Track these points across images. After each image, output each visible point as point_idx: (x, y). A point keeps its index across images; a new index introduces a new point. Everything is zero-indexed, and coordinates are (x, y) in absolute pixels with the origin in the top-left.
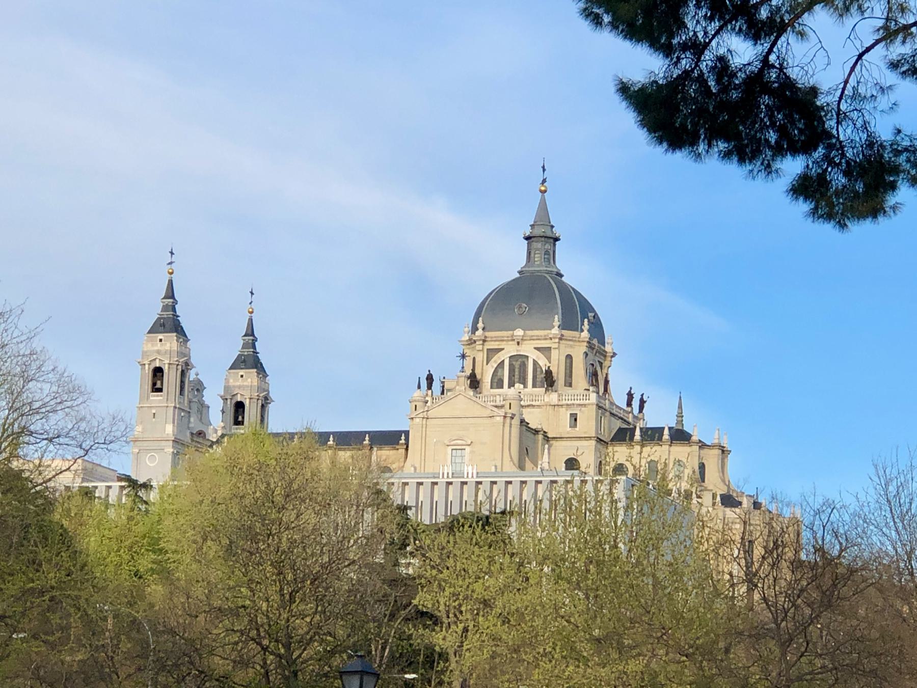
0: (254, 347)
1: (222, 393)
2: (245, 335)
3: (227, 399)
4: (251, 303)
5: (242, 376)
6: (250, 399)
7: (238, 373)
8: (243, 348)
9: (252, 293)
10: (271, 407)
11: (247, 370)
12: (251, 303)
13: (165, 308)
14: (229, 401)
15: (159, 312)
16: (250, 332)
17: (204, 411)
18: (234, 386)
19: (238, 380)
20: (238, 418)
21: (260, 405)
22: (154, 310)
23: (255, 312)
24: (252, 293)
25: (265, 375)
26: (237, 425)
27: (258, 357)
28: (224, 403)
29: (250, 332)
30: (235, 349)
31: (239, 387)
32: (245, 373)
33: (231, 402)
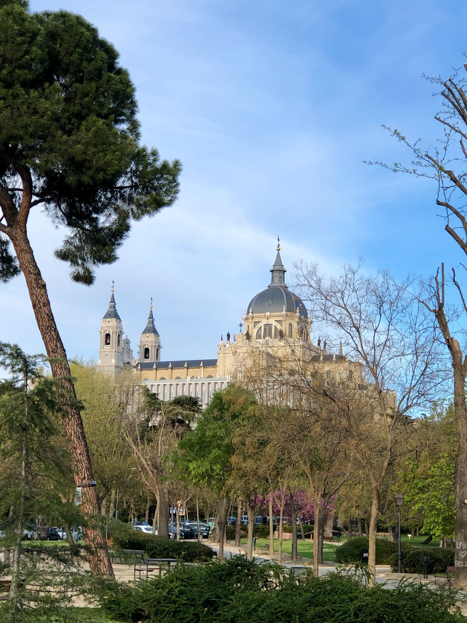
0: (153, 323)
2: (149, 318)
9: (152, 299)
10: (161, 350)
13: (111, 307)
14: (142, 348)
15: (108, 309)
16: (151, 317)
18: (144, 341)
24: (152, 299)
25: (158, 336)
29: (151, 317)
30: (145, 324)
31: (147, 341)
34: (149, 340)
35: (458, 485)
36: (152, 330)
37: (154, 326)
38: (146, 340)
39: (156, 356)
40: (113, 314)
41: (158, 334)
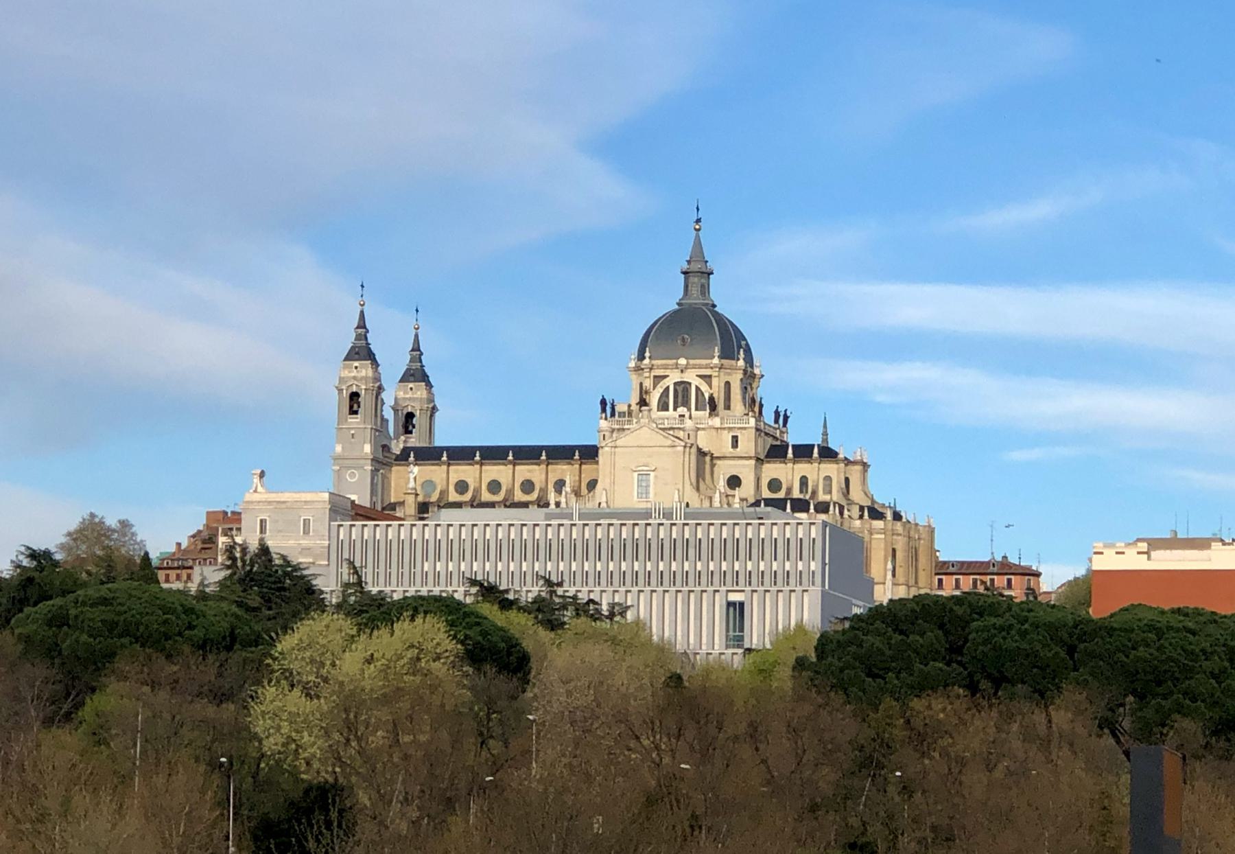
0: (366, 338)
1: (337, 385)
2: (357, 328)
3: (342, 390)
4: (362, 296)
8: (410, 361)
9: (362, 286)
10: (437, 414)
11: (417, 384)
12: (362, 296)
13: (358, 338)
14: (400, 412)
15: (353, 340)
17: (384, 423)
18: (404, 399)
20: (408, 427)
21: (429, 415)
24: (362, 286)
26: (353, 414)
27: (370, 348)
28: (339, 393)
29: (362, 324)
31: (410, 399)
33: (402, 413)
34: (415, 396)
35: (33, 714)
36: (416, 374)
37: (422, 366)
38: (407, 396)
40: (362, 352)
41: (377, 362)
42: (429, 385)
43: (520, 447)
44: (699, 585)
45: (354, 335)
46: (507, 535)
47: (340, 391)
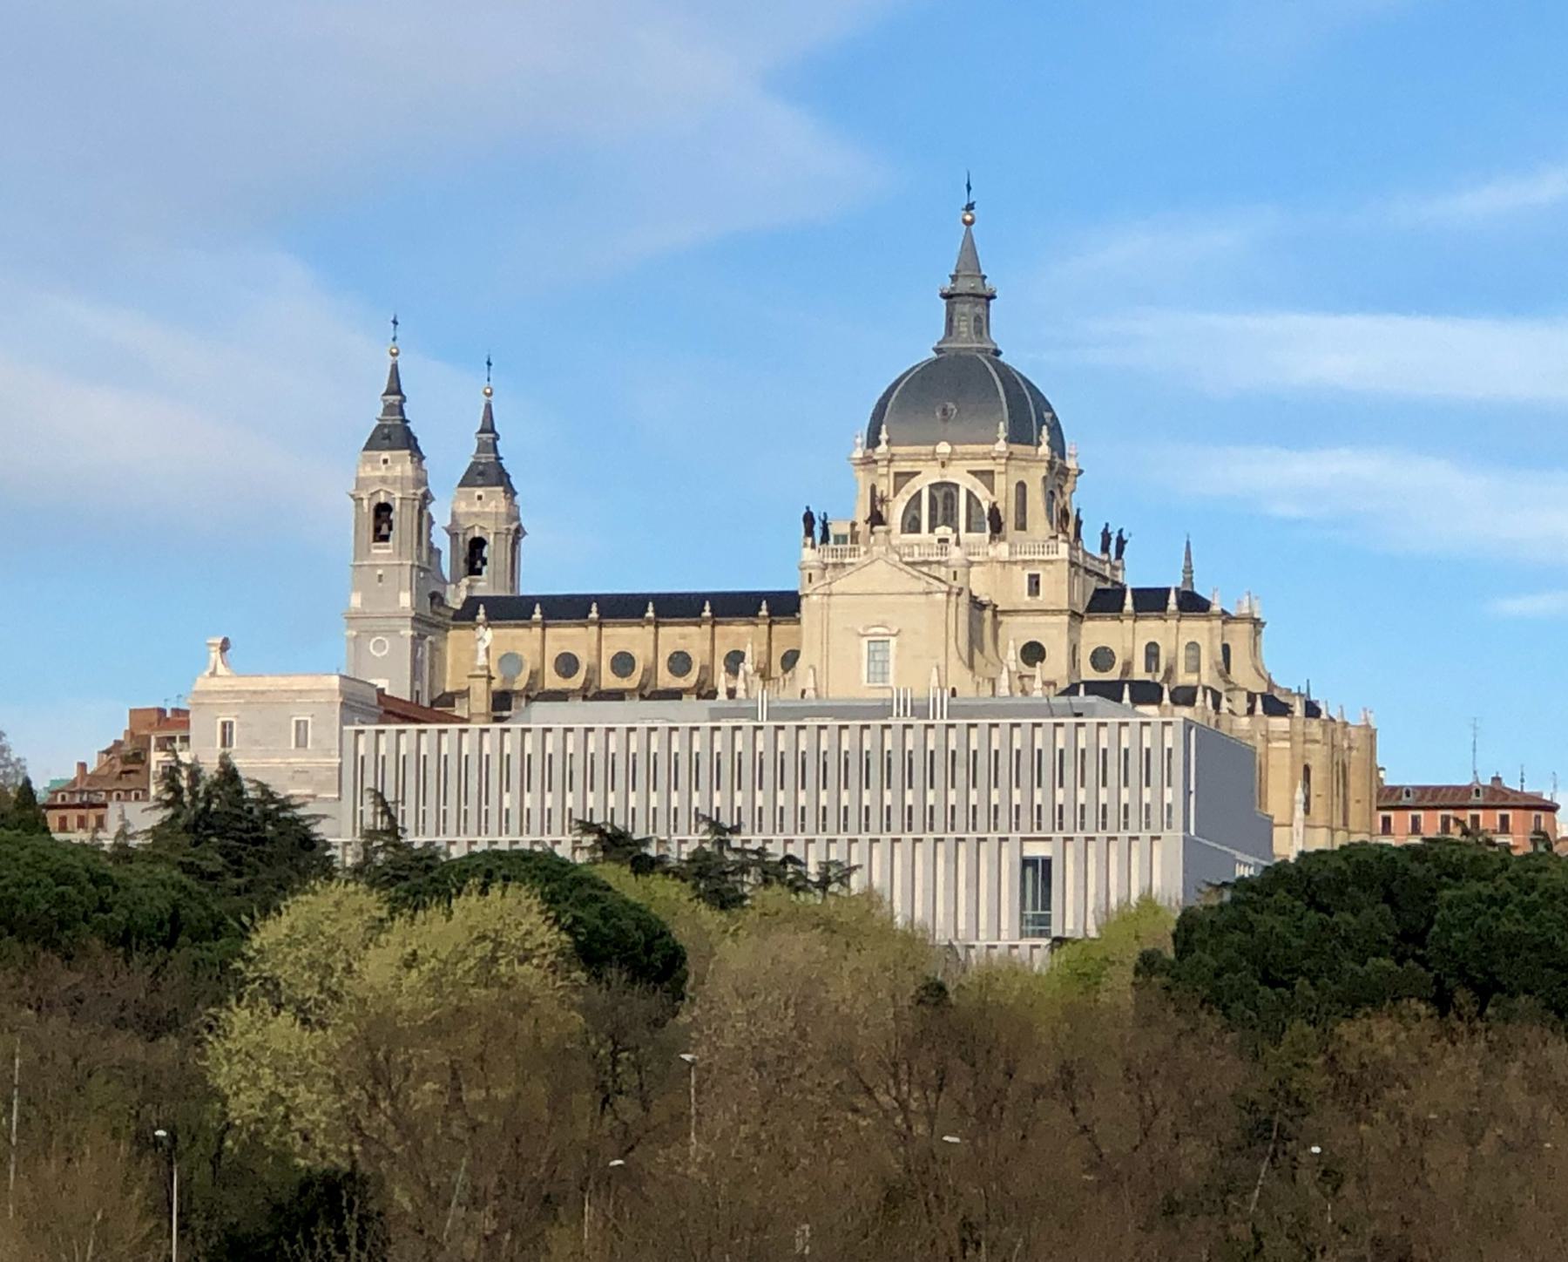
0: (402, 413)
3: (362, 499)
4: (394, 339)
5: (480, 498)
6: (496, 534)
7: (473, 493)
8: (478, 451)
9: (395, 322)
10: (524, 541)
12: (394, 339)
13: (389, 409)
14: (461, 539)
15: (379, 416)
18: (468, 515)
19: (474, 504)
20: (475, 563)
21: (510, 541)
22: (372, 413)
23: (401, 354)
24: (395, 322)
25: (422, 458)
27: (408, 428)
28: (357, 506)
29: (395, 388)
31: (477, 515)
32: (486, 492)
34: (487, 510)
37: (498, 458)
39: (415, 531)
42: (510, 492)
43: (554, 598)
44: (824, 830)
45: (382, 406)
46: (414, 747)
47: (359, 500)
